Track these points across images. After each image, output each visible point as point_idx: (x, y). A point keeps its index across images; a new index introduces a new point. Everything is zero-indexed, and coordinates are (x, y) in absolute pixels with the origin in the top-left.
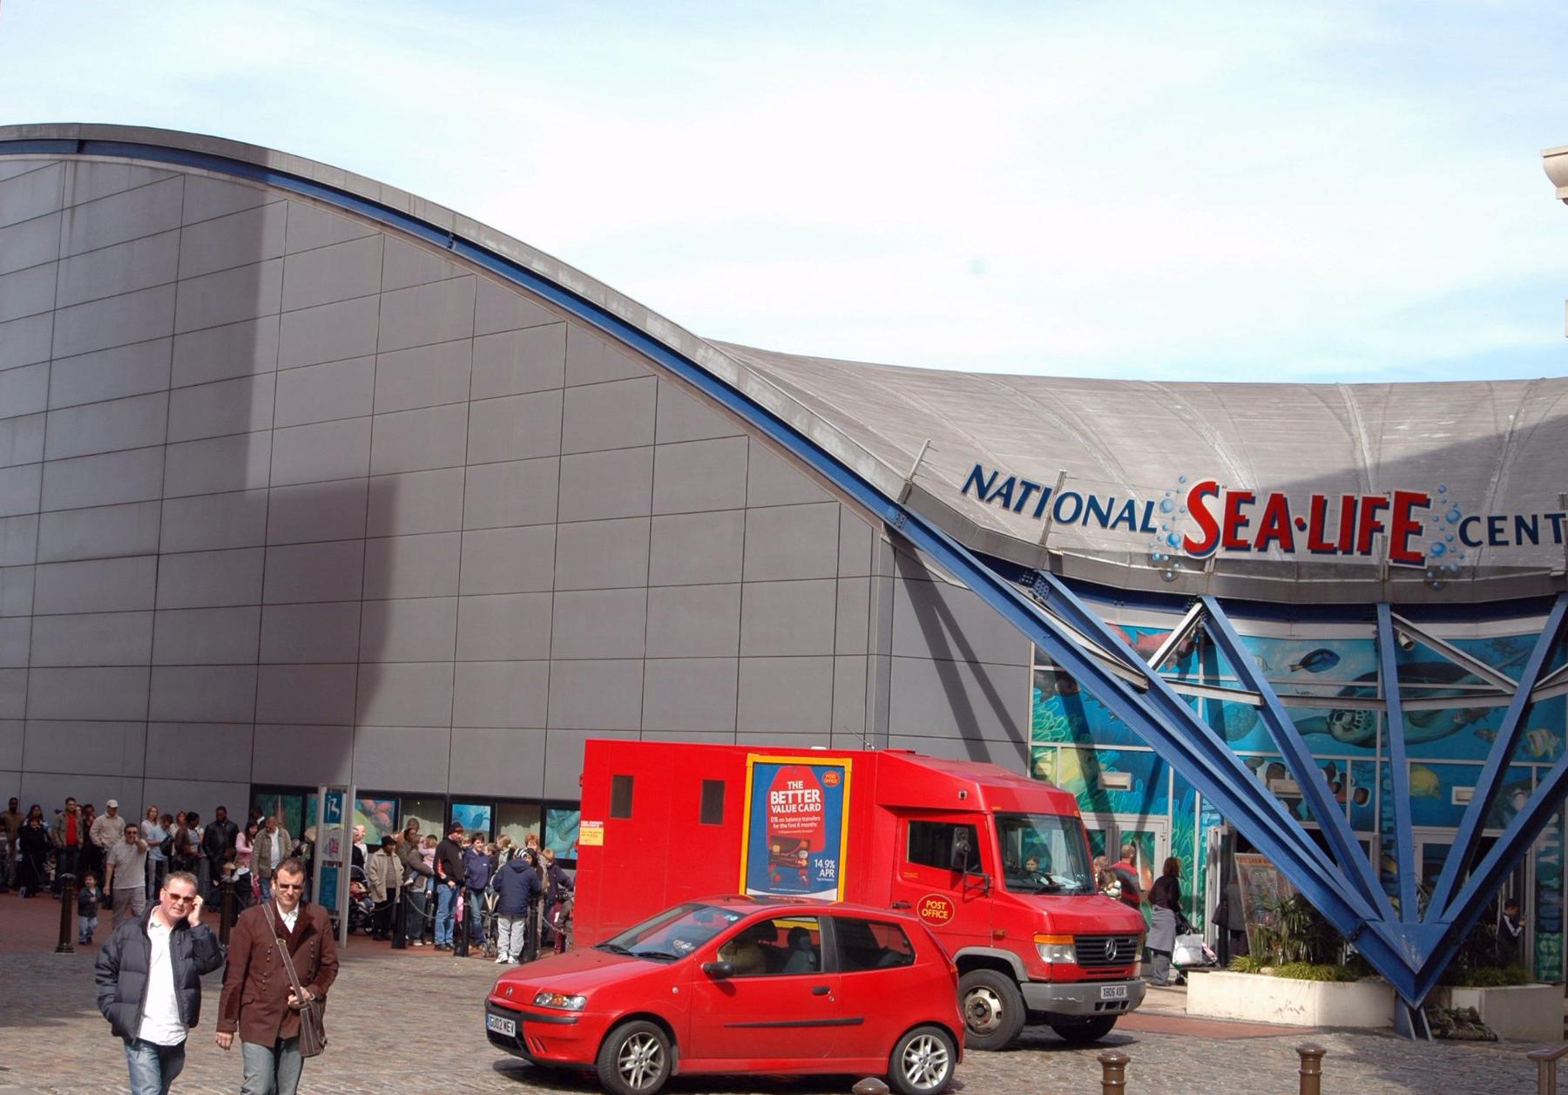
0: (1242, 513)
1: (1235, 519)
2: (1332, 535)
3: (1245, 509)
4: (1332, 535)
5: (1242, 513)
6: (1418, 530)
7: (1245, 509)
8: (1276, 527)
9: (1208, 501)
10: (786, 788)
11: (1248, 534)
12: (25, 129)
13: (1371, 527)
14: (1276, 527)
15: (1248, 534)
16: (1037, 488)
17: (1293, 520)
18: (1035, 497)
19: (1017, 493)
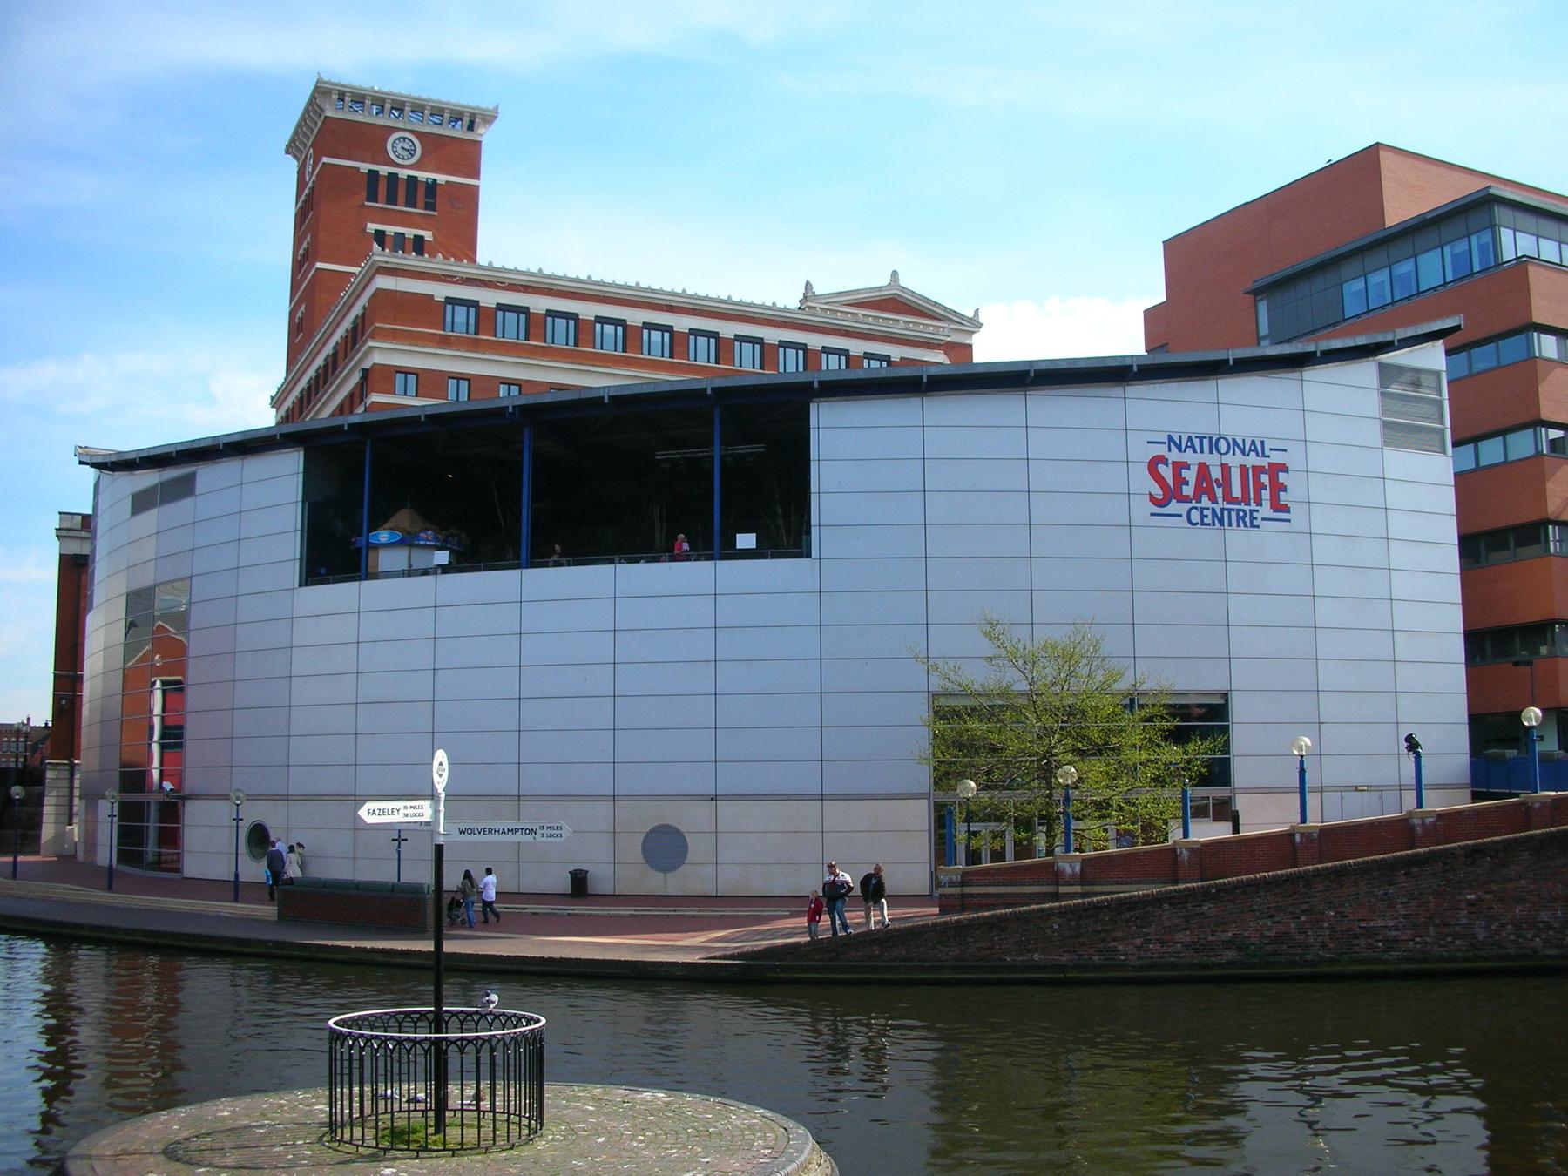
0: (1183, 476)
1: (1180, 481)
2: (1237, 491)
3: (1185, 473)
4: (1237, 491)
5: (1183, 476)
6: (1284, 489)
7: (1185, 473)
8: (1204, 485)
9: (1161, 468)
10: (1084, 861)
11: (1188, 490)
12: (1119, 359)
13: (1259, 487)
14: (1204, 485)
15: (1188, 490)
16: (1205, 438)
17: (1214, 479)
18: (1206, 442)
19: (1196, 442)
